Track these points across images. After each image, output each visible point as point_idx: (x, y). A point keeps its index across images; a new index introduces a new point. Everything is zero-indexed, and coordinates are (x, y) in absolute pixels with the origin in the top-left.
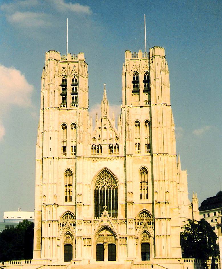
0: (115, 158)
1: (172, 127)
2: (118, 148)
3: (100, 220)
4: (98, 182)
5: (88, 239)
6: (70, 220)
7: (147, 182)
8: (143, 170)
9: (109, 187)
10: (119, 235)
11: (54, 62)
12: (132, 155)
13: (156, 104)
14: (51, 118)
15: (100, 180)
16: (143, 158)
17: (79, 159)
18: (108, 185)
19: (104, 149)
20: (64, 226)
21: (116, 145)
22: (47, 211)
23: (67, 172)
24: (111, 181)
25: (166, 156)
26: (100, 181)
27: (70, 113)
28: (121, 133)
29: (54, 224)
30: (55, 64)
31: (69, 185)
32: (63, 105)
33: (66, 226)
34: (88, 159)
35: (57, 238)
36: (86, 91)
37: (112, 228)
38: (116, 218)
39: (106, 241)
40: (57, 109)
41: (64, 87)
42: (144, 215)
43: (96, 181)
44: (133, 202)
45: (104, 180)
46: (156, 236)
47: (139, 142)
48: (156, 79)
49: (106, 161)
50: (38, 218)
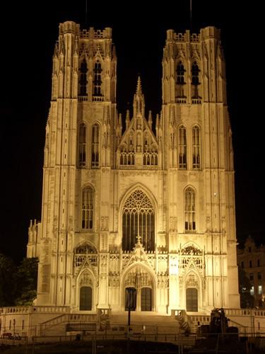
9: (142, 211)
16: (190, 174)
17: (104, 171)
18: (142, 209)
20: (81, 261)
27: (91, 109)
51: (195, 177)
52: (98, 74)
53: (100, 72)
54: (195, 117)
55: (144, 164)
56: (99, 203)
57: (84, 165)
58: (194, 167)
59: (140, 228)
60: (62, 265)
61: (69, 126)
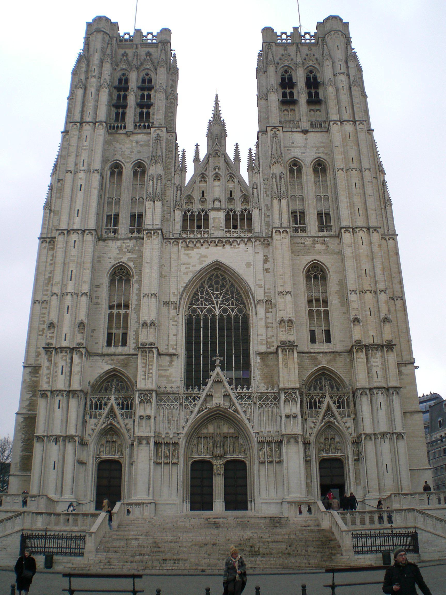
0: (242, 242)
1: (380, 175)
2: (250, 219)
3: (203, 396)
4: (198, 300)
5: (167, 444)
6: (117, 393)
7: (325, 302)
8: (313, 270)
9: (225, 310)
10: (257, 434)
11: (104, 39)
12: (288, 230)
13: (341, 122)
14: (85, 144)
15: (202, 293)
16: (314, 242)
17: (149, 238)
19: (214, 222)
20: (100, 409)
21: (245, 213)
22: (55, 364)
23: (117, 272)
24: (232, 297)
25: (376, 237)
26: (202, 298)
27: (132, 141)
28: (257, 186)
29: (73, 403)
30: (105, 42)
31: (119, 306)
32: (116, 125)
33: (107, 408)
34: (172, 241)
35: (77, 439)
36: (172, 100)
37: (238, 416)
38: (248, 388)
39: (219, 451)
40: (101, 126)
41: (122, 93)
42: (320, 383)
43: (191, 296)
44: (295, 344)
45: (213, 294)
46: (363, 437)
47: (298, 208)
48: (338, 74)
49: (220, 248)
50: (29, 386)
51: (323, 247)
52: (146, 93)
53: (150, 89)
54: (318, 148)
55: (227, 225)
56: (139, 295)
57: (115, 232)
58: (321, 229)
59: (221, 343)
60: (58, 414)
61: (89, 165)
